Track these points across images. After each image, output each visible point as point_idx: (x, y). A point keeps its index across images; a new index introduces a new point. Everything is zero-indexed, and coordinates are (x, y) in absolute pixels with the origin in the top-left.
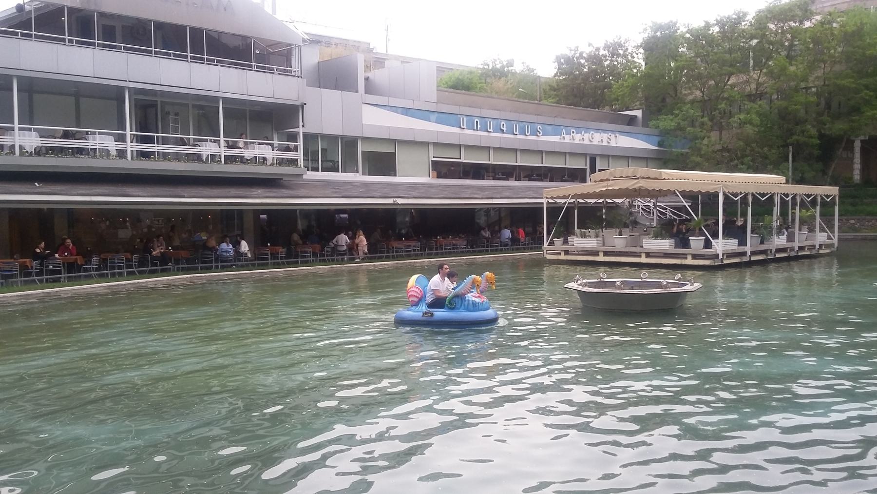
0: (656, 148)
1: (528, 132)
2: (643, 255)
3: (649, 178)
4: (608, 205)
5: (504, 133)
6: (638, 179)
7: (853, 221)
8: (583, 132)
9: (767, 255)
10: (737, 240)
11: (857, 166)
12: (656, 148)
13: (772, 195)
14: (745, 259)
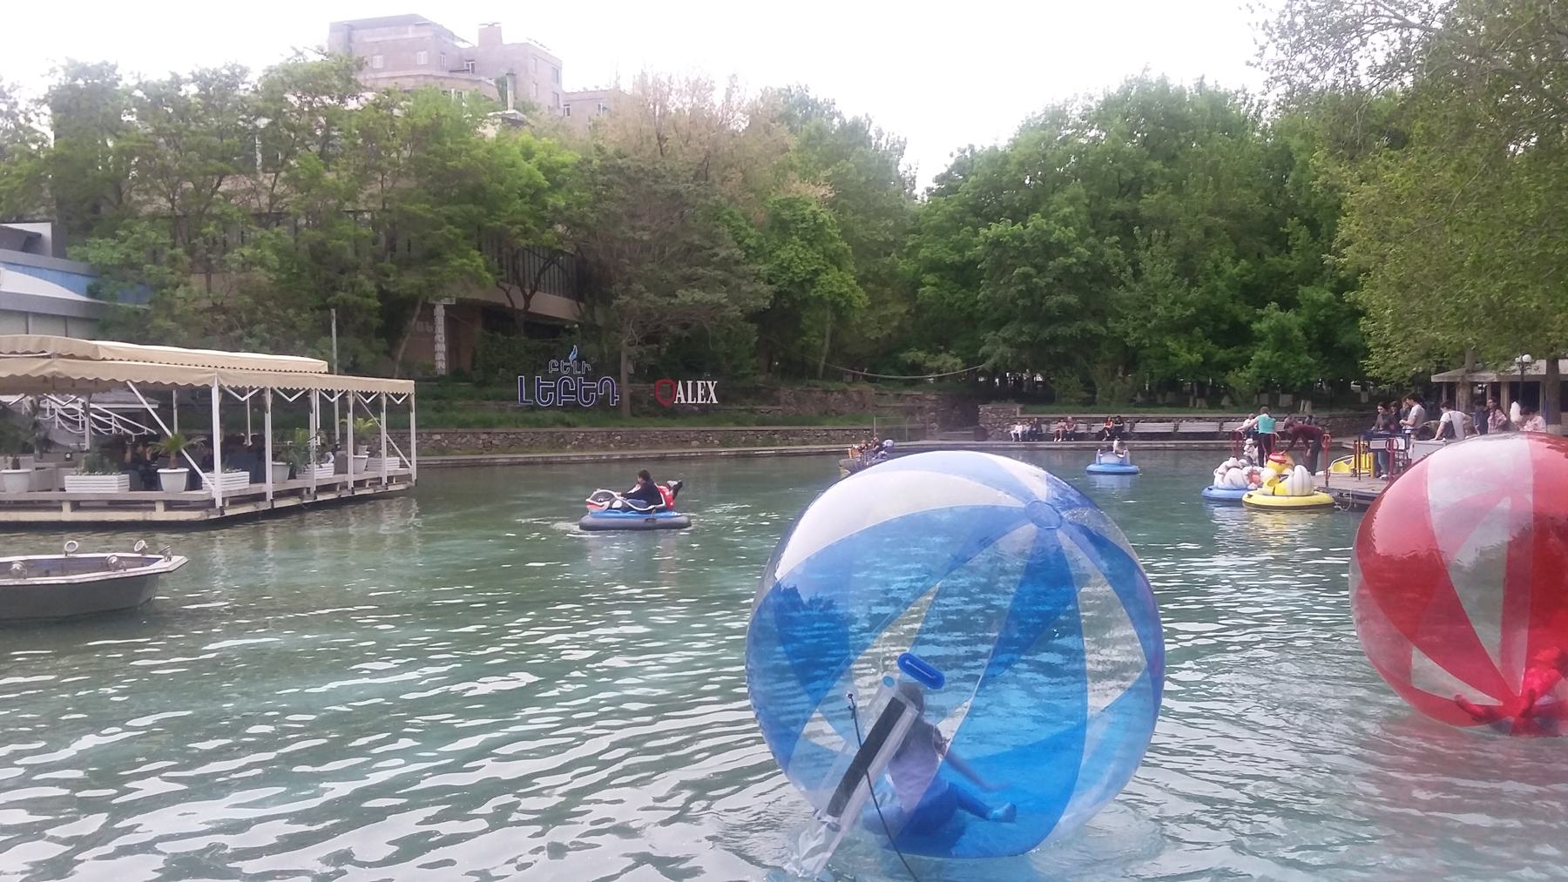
0: (84, 299)
2: (67, 507)
3: (72, 356)
6: (49, 357)
7: (438, 437)
9: (302, 498)
10: (248, 473)
11: (441, 347)
12: (84, 299)
13: (307, 393)
14: (264, 506)
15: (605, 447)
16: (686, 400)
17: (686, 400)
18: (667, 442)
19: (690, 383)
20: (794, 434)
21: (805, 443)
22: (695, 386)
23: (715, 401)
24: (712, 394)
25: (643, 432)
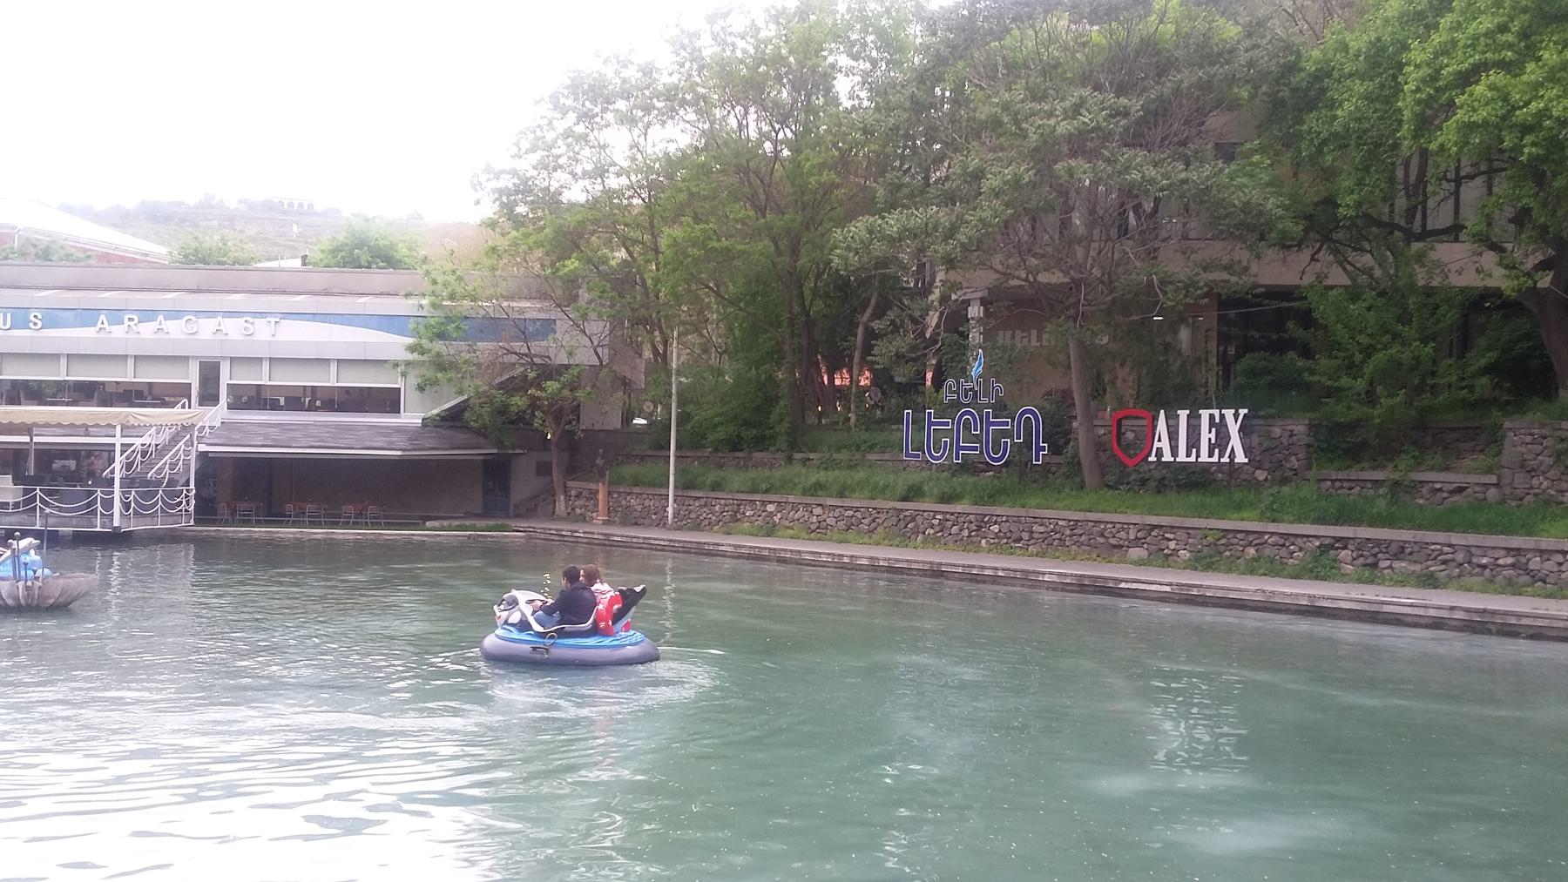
7: (771, 508)
8: (161, 318)
15: (969, 545)
16: (1174, 453)
17: (1174, 453)
18: (1079, 544)
19: (1183, 414)
20: (1400, 552)
21: (1430, 581)
22: (1194, 419)
23: (1241, 458)
24: (1235, 442)
25: (1041, 521)
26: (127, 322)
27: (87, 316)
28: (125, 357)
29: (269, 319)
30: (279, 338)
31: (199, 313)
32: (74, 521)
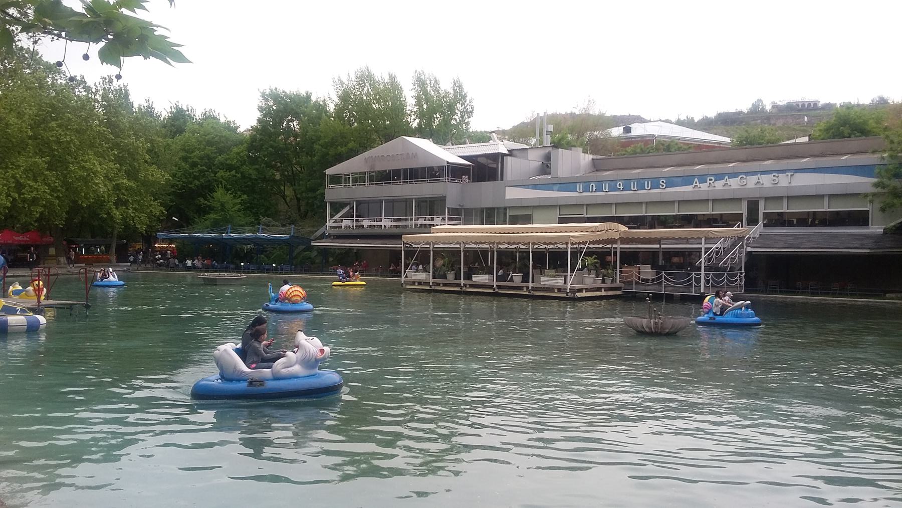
1: (648, 187)
4: (520, 250)
5: (622, 191)
8: (727, 177)
26: (708, 181)
27: (687, 180)
28: (707, 200)
29: (787, 174)
30: (793, 184)
31: (747, 174)
32: (681, 289)
